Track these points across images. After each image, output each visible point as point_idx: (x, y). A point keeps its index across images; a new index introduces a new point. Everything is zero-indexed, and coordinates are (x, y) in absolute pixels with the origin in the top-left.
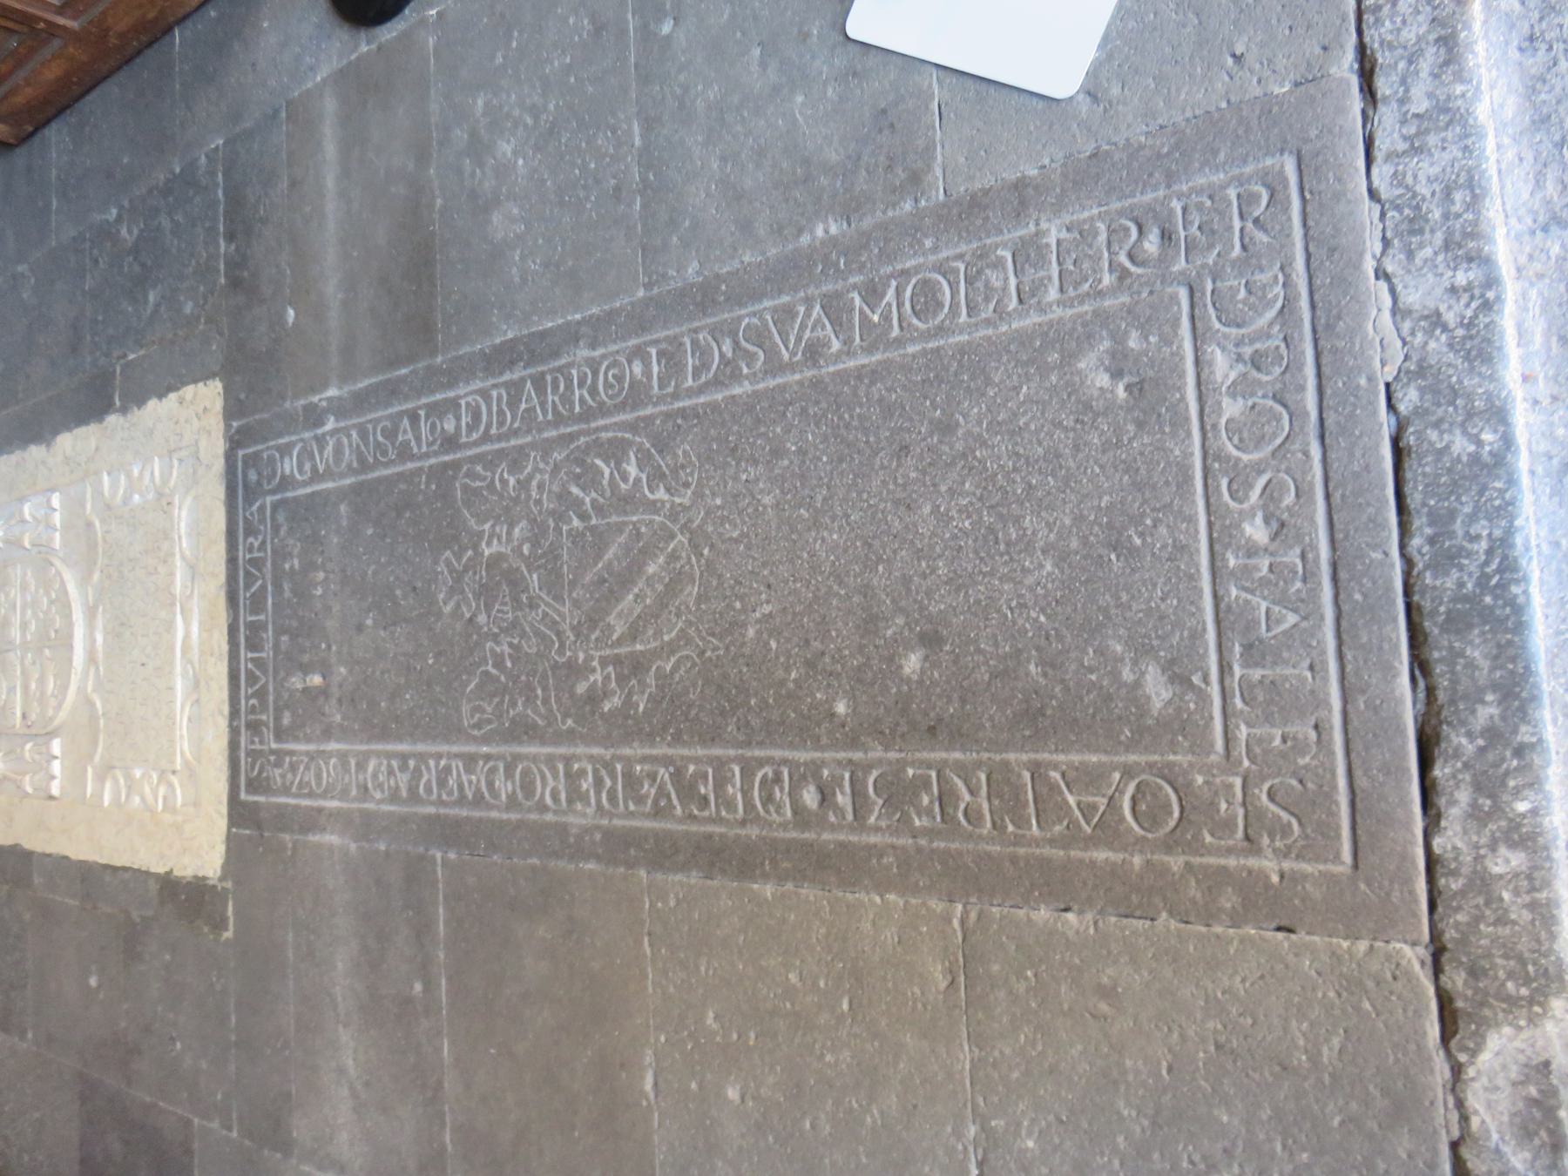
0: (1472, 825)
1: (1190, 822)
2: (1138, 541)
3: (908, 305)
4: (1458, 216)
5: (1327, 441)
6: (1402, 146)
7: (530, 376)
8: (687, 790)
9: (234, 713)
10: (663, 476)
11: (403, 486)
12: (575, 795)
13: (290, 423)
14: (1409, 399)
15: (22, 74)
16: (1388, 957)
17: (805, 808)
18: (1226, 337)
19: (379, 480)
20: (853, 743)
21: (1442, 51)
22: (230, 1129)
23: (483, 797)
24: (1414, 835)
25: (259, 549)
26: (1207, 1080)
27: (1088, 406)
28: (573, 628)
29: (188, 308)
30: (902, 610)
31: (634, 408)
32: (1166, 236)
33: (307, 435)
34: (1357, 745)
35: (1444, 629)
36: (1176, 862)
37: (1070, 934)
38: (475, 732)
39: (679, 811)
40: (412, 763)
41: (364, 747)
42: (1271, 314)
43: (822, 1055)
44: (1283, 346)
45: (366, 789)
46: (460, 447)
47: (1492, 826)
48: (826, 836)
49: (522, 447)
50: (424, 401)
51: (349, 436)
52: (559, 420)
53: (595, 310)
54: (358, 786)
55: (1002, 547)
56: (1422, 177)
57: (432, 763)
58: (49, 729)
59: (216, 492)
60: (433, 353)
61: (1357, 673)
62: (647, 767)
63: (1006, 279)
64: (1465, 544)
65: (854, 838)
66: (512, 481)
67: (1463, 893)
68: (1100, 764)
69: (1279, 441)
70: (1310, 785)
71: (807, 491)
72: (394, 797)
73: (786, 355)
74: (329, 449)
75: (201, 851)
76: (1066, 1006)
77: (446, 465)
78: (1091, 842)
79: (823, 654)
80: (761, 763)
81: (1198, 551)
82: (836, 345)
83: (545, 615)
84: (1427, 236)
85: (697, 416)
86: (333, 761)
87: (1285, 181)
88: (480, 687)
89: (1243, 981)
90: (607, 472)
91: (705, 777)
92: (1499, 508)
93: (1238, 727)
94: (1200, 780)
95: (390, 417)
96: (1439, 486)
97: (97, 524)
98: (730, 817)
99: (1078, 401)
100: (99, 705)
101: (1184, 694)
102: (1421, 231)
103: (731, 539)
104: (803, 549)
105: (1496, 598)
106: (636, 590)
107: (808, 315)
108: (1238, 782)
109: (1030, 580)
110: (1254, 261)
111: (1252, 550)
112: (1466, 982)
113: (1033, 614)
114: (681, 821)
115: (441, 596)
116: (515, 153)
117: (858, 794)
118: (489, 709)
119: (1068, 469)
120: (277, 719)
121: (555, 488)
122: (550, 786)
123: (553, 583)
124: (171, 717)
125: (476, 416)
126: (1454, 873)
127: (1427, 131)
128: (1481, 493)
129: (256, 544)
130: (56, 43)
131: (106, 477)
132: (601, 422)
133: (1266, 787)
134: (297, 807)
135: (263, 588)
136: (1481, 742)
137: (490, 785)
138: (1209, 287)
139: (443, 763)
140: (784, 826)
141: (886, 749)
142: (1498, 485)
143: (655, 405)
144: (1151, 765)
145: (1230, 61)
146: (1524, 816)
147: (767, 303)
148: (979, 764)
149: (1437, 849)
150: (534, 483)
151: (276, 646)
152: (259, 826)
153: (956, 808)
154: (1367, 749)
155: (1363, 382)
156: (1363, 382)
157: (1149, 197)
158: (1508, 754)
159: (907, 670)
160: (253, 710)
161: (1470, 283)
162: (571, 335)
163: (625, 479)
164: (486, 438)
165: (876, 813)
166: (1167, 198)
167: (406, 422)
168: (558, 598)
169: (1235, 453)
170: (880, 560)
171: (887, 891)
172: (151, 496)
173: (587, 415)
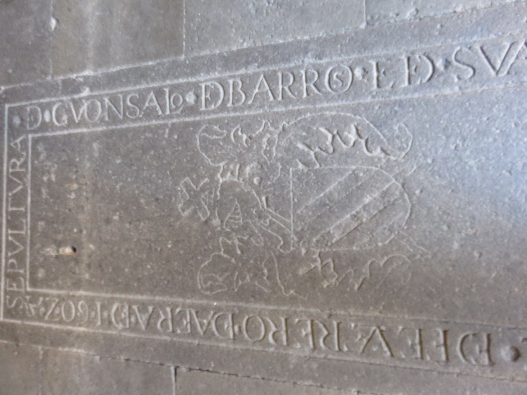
11: (149, 135)
13: (51, 89)
19: (128, 130)
25: (21, 166)
28: (296, 233)
33: (65, 98)
38: (208, 293)
41: (109, 295)
50: (168, 82)
60: (178, 52)
66: (245, 137)
72: (135, 328)
83: (272, 223)
95: (140, 92)
115: (180, 206)
121: (283, 143)
125: (214, 95)
129: (18, 163)
134: (49, 330)
150: (265, 140)
151: (34, 228)
160: (12, 266)
162: (303, 49)
167: (152, 95)
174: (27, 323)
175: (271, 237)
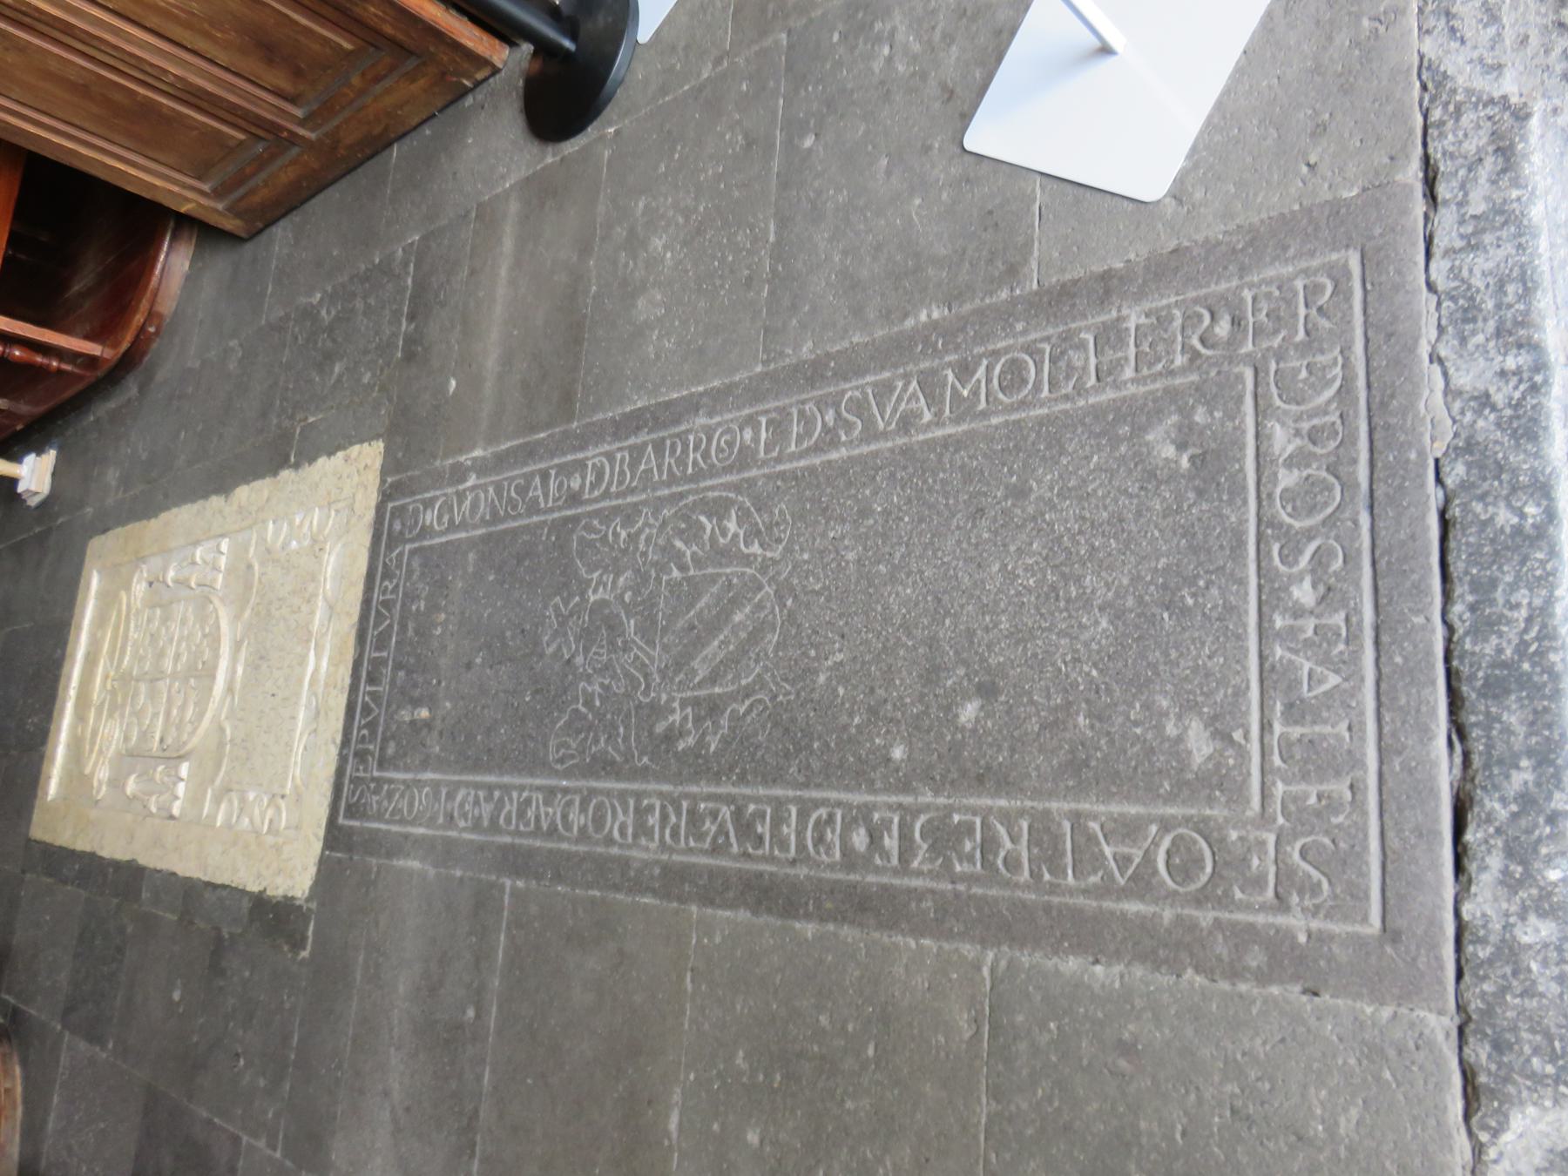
0: (1502, 892)
1: (1222, 877)
2: (1190, 601)
3: (995, 382)
4: (1510, 306)
5: (1376, 511)
6: (1459, 244)
7: (653, 441)
8: (745, 828)
9: (346, 742)
10: (759, 532)
11: (526, 538)
12: (642, 830)
13: (438, 479)
14: (1456, 472)
15: (263, 175)
16: (1412, 1025)
17: (853, 850)
18: (1286, 412)
19: (505, 532)
20: (906, 788)
21: (1500, 160)
22: (275, 1149)
23: (556, 830)
24: (1443, 900)
26: (1220, 1147)
27: (1152, 475)
28: (660, 671)
29: (366, 378)
30: (965, 663)
31: (739, 471)
32: (1236, 322)
33: (450, 490)
34: (1392, 806)
35: (1482, 695)
36: (1206, 917)
37: (1096, 987)
38: (559, 767)
39: (735, 849)
40: (497, 794)
41: (456, 778)
42: (1329, 393)
43: (843, 1101)
44: (1339, 422)
45: (452, 817)
46: (582, 503)
47: (1523, 894)
48: (871, 878)
49: (636, 505)
50: (556, 461)
51: (486, 492)
52: (672, 480)
53: (716, 383)
54: (446, 815)
55: (1062, 604)
56: (1477, 271)
57: (515, 795)
58: (182, 752)
59: (362, 539)
60: (570, 420)
61: (1394, 734)
62: (711, 805)
63: (1087, 359)
64: (1506, 612)
65: (896, 882)
66: (623, 534)
67: (1490, 961)
68: (1138, 817)
69: (1330, 510)
70: (1342, 845)
71: (887, 549)
72: (476, 826)
73: (881, 425)
74: (468, 503)
75: (291, 872)
76: (1085, 1062)
77: (566, 520)
78: (1124, 894)
79: (886, 701)
80: (817, 804)
81: (1246, 612)
82: (927, 416)
83: (637, 657)
84: (1480, 324)
85: (796, 478)
86: (426, 789)
87: (1348, 274)
88: (568, 724)
89: (1264, 1043)
90: (709, 527)
91: (763, 817)
92: (1539, 578)
93: (1274, 784)
94: (1234, 835)
95: (524, 475)
96: (1482, 555)
97: (256, 567)
98: (783, 856)
99: (1144, 470)
100: (228, 732)
101: (1224, 750)
102: (1474, 320)
103: (813, 591)
104: (878, 602)
105: (1533, 665)
106: (722, 637)
107: (905, 389)
108: (1271, 839)
109: (1086, 636)
110: (1316, 344)
111: (1298, 612)
112: (1489, 1056)
113: (1086, 668)
114: (735, 858)
116: (665, 247)
117: (905, 836)
118: (574, 745)
119: (1130, 532)
120: (382, 749)
121: (661, 542)
122: (620, 821)
123: (648, 630)
124: (289, 745)
126: (1483, 941)
127: (1484, 231)
128: (1523, 562)
130: (295, 151)
131: (271, 525)
132: (709, 483)
133: (1298, 845)
134: (389, 832)
135: (390, 626)
136: (1514, 808)
137: (565, 817)
138: (1273, 366)
139: (525, 794)
140: (831, 867)
141: (937, 793)
142: (1540, 555)
143: (759, 468)
144: (1187, 820)
145: (1305, 169)
146: (1555, 885)
147: (869, 379)
148: (1022, 813)
149: (1466, 916)
150: (643, 537)
151: (393, 683)
152: (350, 849)
153: (996, 855)
154: (1400, 810)
155: (1413, 456)
156: (1413, 456)
157: (1223, 286)
158: (1541, 820)
159: (963, 719)
161: (1519, 367)
162: (692, 406)
163: (724, 533)
164: (606, 495)
165: (920, 858)
166: (1240, 288)
167: (538, 479)
168: (651, 643)
169: (1288, 520)
170: (947, 613)
171: (922, 936)
172: (306, 543)
173: (699, 475)
174: (367, 825)
175: (632, 679)
